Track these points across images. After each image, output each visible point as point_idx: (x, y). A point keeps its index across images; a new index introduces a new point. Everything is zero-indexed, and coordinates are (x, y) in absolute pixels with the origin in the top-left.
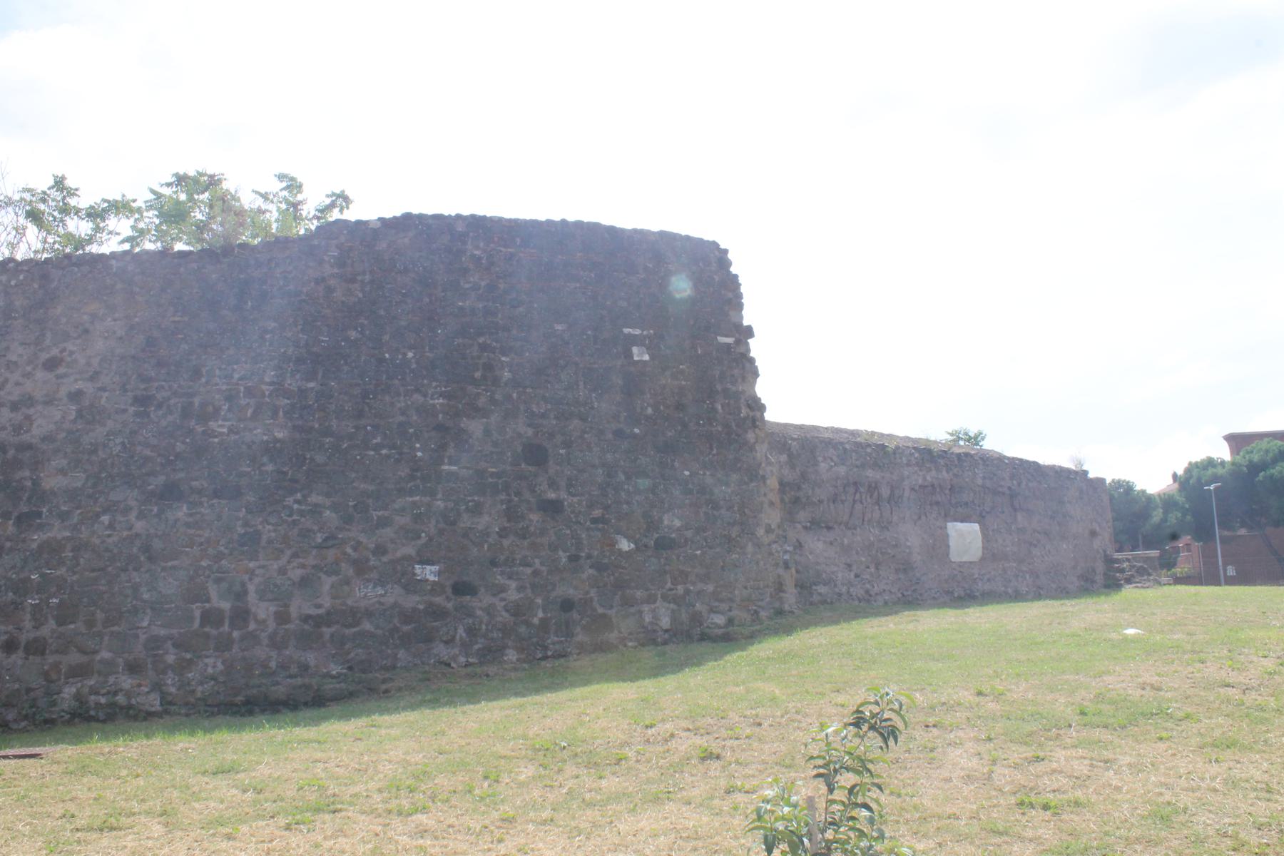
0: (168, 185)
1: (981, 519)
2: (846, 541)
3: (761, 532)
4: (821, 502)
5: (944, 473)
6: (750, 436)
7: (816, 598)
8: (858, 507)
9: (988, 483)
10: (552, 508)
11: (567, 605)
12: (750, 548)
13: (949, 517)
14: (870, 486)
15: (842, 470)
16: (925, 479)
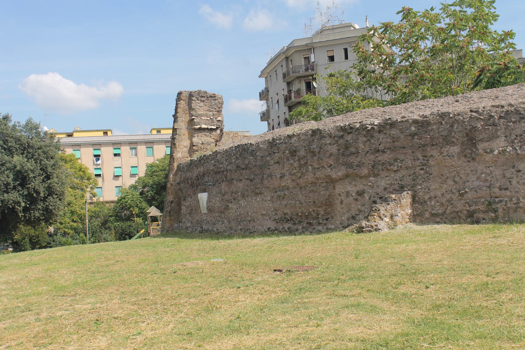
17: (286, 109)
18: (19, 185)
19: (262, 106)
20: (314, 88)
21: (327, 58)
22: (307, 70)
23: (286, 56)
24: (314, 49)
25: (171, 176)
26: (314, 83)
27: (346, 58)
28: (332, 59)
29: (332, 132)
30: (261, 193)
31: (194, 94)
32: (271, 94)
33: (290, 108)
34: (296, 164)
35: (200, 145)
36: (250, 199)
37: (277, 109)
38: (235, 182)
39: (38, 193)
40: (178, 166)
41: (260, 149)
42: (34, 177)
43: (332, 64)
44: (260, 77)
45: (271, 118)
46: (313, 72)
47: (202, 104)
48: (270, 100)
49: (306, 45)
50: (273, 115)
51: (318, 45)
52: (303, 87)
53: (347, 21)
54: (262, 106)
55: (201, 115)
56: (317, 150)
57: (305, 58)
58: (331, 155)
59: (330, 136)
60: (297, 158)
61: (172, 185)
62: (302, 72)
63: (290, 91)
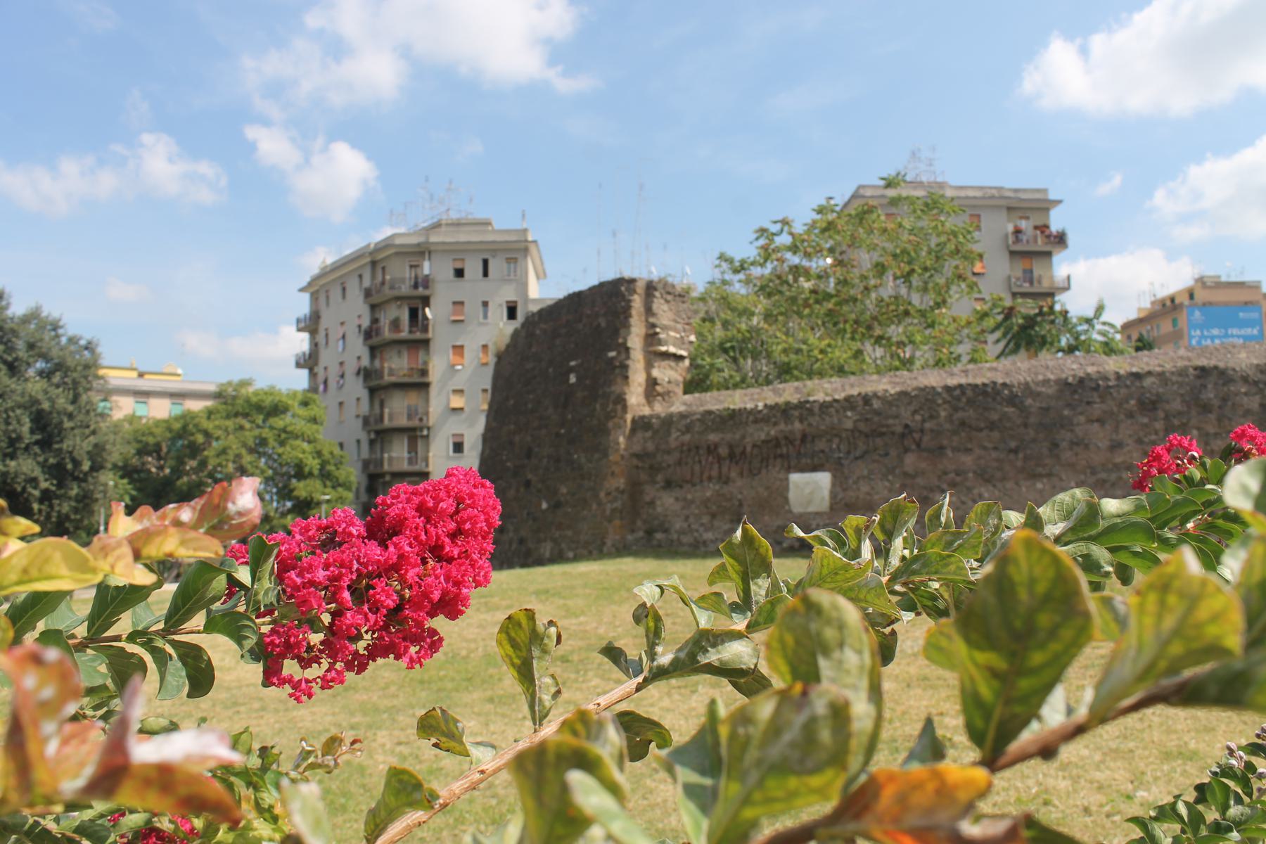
0: (757, 239)
1: (837, 469)
2: (689, 497)
3: (602, 495)
4: (669, 466)
5: (797, 425)
6: (610, 424)
7: (655, 542)
8: (697, 468)
9: (862, 426)
10: (528, 484)
11: (522, 541)
12: (594, 506)
13: (790, 469)
14: (709, 447)
15: (687, 437)
16: (768, 434)
18: (37, 443)
19: (301, 343)
20: (425, 318)
21: (452, 272)
22: (416, 286)
23: (375, 260)
25: (621, 439)
26: (427, 310)
27: (486, 274)
28: (459, 273)
29: (1250, 373)
30: (1049, 475)
31: (660, 286)
32: (324, 323)
33: (373, 350)
34: (1159, 425)
35: (665, 384)
36: (1009, 485)
37: (340, 349)
38: (949, 453)
39: (77, 463)
40: (633, 421)
41: (1036, 395)
42: (73, 429)
43: (459, 283)
44: (302, 290)
45: (322, 363)
46: (427, 292)
47: (665, 307)
48: (322, 333)
49: (419, 245)
50: (327, 358)
51: (440, 248)
53: (480, 215)
54: (301, 343)
55: (665, 328)
56: (1216, 403)
57: (411, 266)
58: (1247, 412)
59: (1245, 379)
60: (1161, 414)
61: (623, 457)
62: (405, 289)
63: (375, 321)
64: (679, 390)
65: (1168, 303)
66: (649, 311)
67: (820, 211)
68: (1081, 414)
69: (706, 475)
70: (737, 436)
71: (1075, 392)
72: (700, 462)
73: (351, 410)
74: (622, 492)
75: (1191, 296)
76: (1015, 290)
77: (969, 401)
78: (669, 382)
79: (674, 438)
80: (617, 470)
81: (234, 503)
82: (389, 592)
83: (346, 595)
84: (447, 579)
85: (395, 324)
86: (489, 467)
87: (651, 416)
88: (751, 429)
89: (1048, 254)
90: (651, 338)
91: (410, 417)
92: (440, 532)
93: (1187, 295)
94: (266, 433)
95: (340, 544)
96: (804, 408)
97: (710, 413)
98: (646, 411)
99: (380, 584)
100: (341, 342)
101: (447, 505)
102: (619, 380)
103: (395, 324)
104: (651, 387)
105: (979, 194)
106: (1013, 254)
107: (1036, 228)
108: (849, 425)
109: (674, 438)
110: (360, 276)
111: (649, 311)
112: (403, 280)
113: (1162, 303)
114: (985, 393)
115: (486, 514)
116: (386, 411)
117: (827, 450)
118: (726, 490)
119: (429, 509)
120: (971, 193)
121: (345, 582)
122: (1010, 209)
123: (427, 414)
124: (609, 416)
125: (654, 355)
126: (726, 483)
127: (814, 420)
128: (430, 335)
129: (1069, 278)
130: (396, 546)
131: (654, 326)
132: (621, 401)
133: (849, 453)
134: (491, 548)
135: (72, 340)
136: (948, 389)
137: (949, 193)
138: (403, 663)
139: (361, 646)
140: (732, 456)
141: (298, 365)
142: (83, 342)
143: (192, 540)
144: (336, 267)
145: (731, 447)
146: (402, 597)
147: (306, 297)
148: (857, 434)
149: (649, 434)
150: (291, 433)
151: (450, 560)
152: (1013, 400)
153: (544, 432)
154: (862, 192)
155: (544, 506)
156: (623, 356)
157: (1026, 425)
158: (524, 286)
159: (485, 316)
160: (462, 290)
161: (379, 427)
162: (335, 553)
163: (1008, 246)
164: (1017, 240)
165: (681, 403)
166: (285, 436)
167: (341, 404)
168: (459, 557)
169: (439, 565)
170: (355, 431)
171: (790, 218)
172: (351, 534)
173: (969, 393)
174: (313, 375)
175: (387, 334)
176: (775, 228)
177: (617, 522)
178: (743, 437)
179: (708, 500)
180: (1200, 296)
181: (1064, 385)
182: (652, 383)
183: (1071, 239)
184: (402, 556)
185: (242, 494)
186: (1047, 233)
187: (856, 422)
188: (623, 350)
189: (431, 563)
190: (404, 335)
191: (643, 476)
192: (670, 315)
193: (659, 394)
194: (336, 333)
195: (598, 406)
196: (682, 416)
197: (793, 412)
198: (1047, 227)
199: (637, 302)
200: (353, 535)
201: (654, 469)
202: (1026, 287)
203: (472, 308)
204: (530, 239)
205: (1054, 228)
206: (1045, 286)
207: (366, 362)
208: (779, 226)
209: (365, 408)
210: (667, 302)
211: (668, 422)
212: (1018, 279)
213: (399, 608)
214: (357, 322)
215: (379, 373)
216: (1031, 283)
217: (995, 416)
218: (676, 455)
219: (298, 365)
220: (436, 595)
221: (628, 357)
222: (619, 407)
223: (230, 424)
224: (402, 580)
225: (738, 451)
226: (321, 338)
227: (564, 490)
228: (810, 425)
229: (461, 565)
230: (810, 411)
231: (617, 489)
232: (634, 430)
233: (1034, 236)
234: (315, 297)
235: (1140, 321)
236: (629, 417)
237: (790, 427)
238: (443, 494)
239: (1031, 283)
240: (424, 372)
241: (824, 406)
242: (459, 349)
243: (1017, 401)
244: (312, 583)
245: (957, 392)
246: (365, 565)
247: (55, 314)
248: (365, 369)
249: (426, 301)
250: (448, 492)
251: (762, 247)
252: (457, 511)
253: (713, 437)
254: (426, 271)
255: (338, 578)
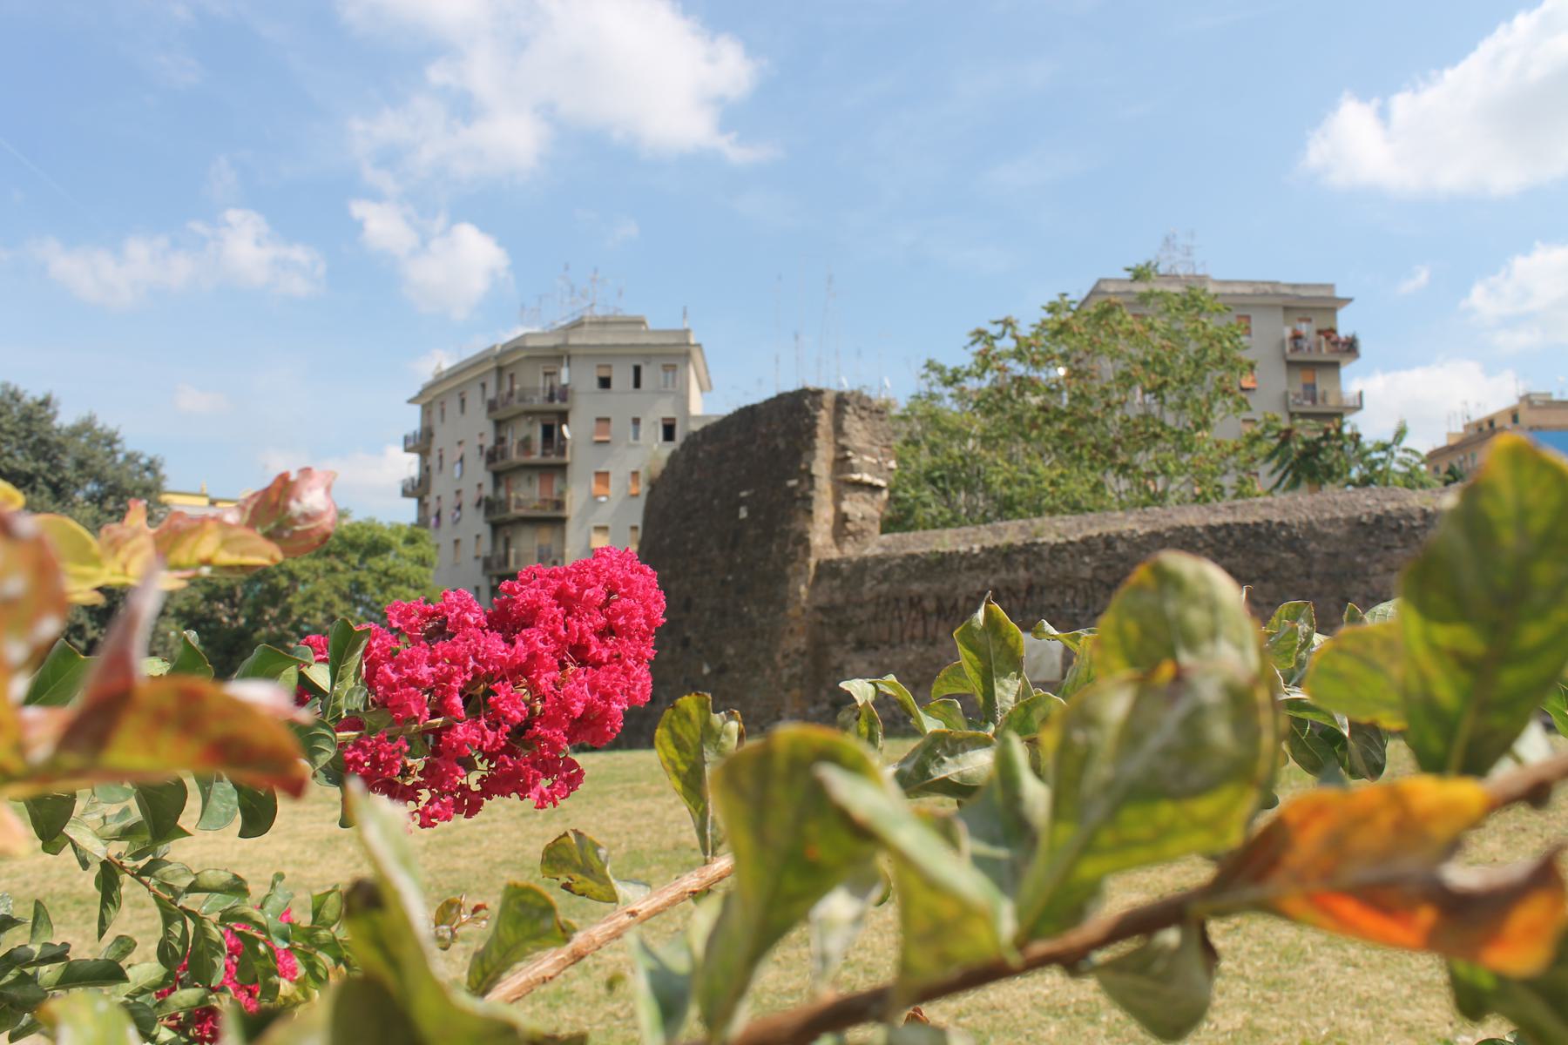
0: (973, 343)
2: (886, 661)
3: (778, 657)
5: (1022, 573)
9: (1102, 574)
10: (686, 643)
12: (768, 672)
14: (911, 599)
15: (885, 587)
17: (486, 479)
19: (410, 465)
20: (562, 438)
21: (595, 382)
22: (551, 398)
23: (502, 365)
24: (569, 358)
25: (803, 589)
26: (565, 428)
27: (637, 384)
28: (605, 383)
31: (852, 399)
33: (498, 477)
37: (457, 474)
40: (818, 566)
44: (411, 401)
46: (564, 406)
47: (859, 425)
48: (435, 455)
49: (555, 347)
51: (581, 351)
52: (537, 435)
53: (630, 310)
54: (410, 465)
55: (859, 451)
57: (546, 374)
61: (804, 610)
62: (538, 402)
63: (500, 440)
64: (876, 529)
65: (1486, 427)
66: (839, 430)
67: (1052, 309)
68: (1378, 561)
69: (907, 635)
70: (947, 587)
71: (1370, 534)
72: (900, 618)
73: (469, 550)
74: (803, 654)
75: (1515, 419)
76: (1293, 409)
77: (1237, 545)
78: (863, 518)
79: (869, 587)
80: (797, 627)
81: (298, 501)
82: (516, 700)
83: (458, 701)
84: (593, 689)
85: (525, 445)
86: (650, 551)
87: (840, 561)
88: (963, 578)
89: (1335, 365)
90: (842, 463)
91: (541, 559)
92: (585, 627)
93: (1509, 418)
94: (363, 576)
95: (451, 636)
96: (1031, 552)
97: (913, 556)
98: (834, 554)
99: (504, 690)
100: (458, 467)
101: (596, 593)
102: (801, 515)
103: (525, 445)
104: (841, 525)
105: (1248, 290)
106: (1291, 365)
107: (1320, 332)
108: (1087, 573)
109: (869, 587)
110: (483, 386)
111: (839, 430)
112: (535, 391)
113: (1479, 426)
114: (1257, 535)
115: (647, 608)
116: (512, 551)
117: (1059, 604)
118: (932, 652)
119: (570, 597)
120: (1239, 289)
121: (457, 684)
122: (1287, 309)
123: (562, 555)
124: (788, 560)
125: (845, 485)
126: (932, 644)
127: (1043, 567)
128: (568, 458)
129: (1361, 394)
130: (526, 641)
131: (844, 448)
132: (803, 540)
133: (1086, 608)
134: (650, 653)
135: (131, 458)
136: (1210, 529)
137: (1212, 289)
138: (530, 802)
139: (473, 780)
140: (940, 611)
141: (405, 494)
142: (143, 461)
143: (238, 539)
144: (455, 373)
145: (939, 599)
146: (532, 711)
147: (416, 410)
148: (1096, 585)
149: (837, 583)
150: (394, 576)
151: (598, 664)
152: (1292, 543)
153: (707, 578)
154: (1103, 287)
155: (706, 670)
156: (806, 485)
157: (1308, 575)
158: (684, 399)
159: (636, 437)
160: (607, 403)
161: (502, 571)
162: (441, 647)
163: (1284, 356)
164: (1296, 348)
165: (876, 545)
166: (388, 579)
167: (457, 542)
168: (609, 662)
169: (582, 670)
170: (474, 574)
171: (1014, 318)
172: (466, 623)
173: (1237, 534)
174: (422, 505)
175: (515, 456)
176: (995, 330)
177: (796, 692)
178: (955, 588)
179: (910, 665)
180: (1526, 417)
181: (1357, 524)
182: (842, 519)
183: (1363, 347)
184: (534, 656)
185: (310, 489)
186: (1334, 338)
187: (1095, 569)
188: (806, 478)
189: (572, 668)
190: (536, 457)
191: (829, 635)
192: (865, 435)
193: (850, 533)
194: (452, 455)
195: (774, 548)
196: (879, 560)
197: (1016, 556)
198: (1333, 331)
199: (824, 419)
200: (469, 625)
201: (843, 627)
202: (1308, 406)
203: (620, 425)
204: (692, 341)
205: (1343, 331)
206: (1332, 403)
207: (488, 491)
208: (998, 329)
209: (486, 547)
210: (862, 419)
211: (861, 567)
212: (1297, 396)
213: (528, 724)
214: (478, 442)
215: (505, 505)
216: (1314, 401)
217: (1269, 564)
218: (871, 609)
219: (405, 494)
220: (579, 708)
221: (812, 487)
222: (800, 549)
223: (320, 564)
224: (533, 687)
225: (948, 604)
226: (433, 460)
227: (730, 651)
228: (1038, 573)
229: (610, 672)
230: (1039, 556)
231: (797, 651)
232: (818, 578)
233: (1316, 342)
234: (427, 411)
235: (1449, 450)
236: (812, 561)
237: (1012, 576)
238: (589, 578)
239: (1314, 401)
240: (560, 505)
241: (1056, 549)
242: (602, 477)
243: (1298, 544)
244: (412, 681)
245: (1222, 533)
246: (484, 663)
247: (111, 426)
248: (487, 499)
249: (563, 417)
250: (597, 576)
251: (979, 353)
252: (607, 603)
253: (917, 587)
254: (564, 379)
255: (449, 678)
